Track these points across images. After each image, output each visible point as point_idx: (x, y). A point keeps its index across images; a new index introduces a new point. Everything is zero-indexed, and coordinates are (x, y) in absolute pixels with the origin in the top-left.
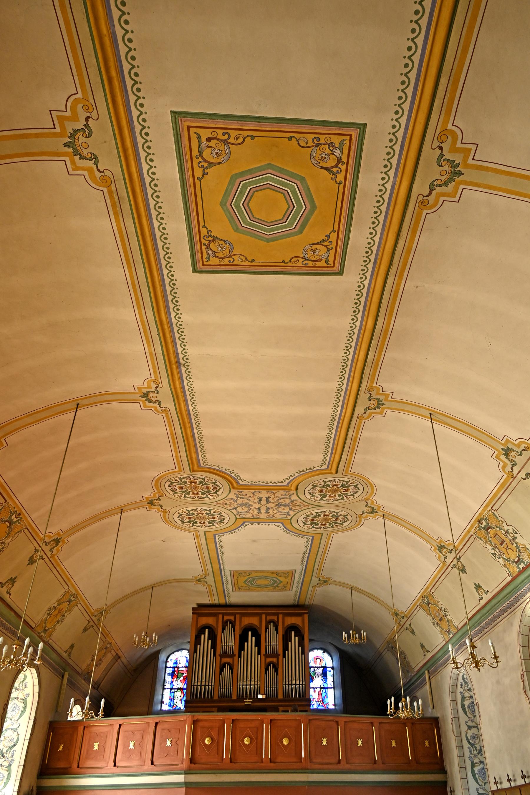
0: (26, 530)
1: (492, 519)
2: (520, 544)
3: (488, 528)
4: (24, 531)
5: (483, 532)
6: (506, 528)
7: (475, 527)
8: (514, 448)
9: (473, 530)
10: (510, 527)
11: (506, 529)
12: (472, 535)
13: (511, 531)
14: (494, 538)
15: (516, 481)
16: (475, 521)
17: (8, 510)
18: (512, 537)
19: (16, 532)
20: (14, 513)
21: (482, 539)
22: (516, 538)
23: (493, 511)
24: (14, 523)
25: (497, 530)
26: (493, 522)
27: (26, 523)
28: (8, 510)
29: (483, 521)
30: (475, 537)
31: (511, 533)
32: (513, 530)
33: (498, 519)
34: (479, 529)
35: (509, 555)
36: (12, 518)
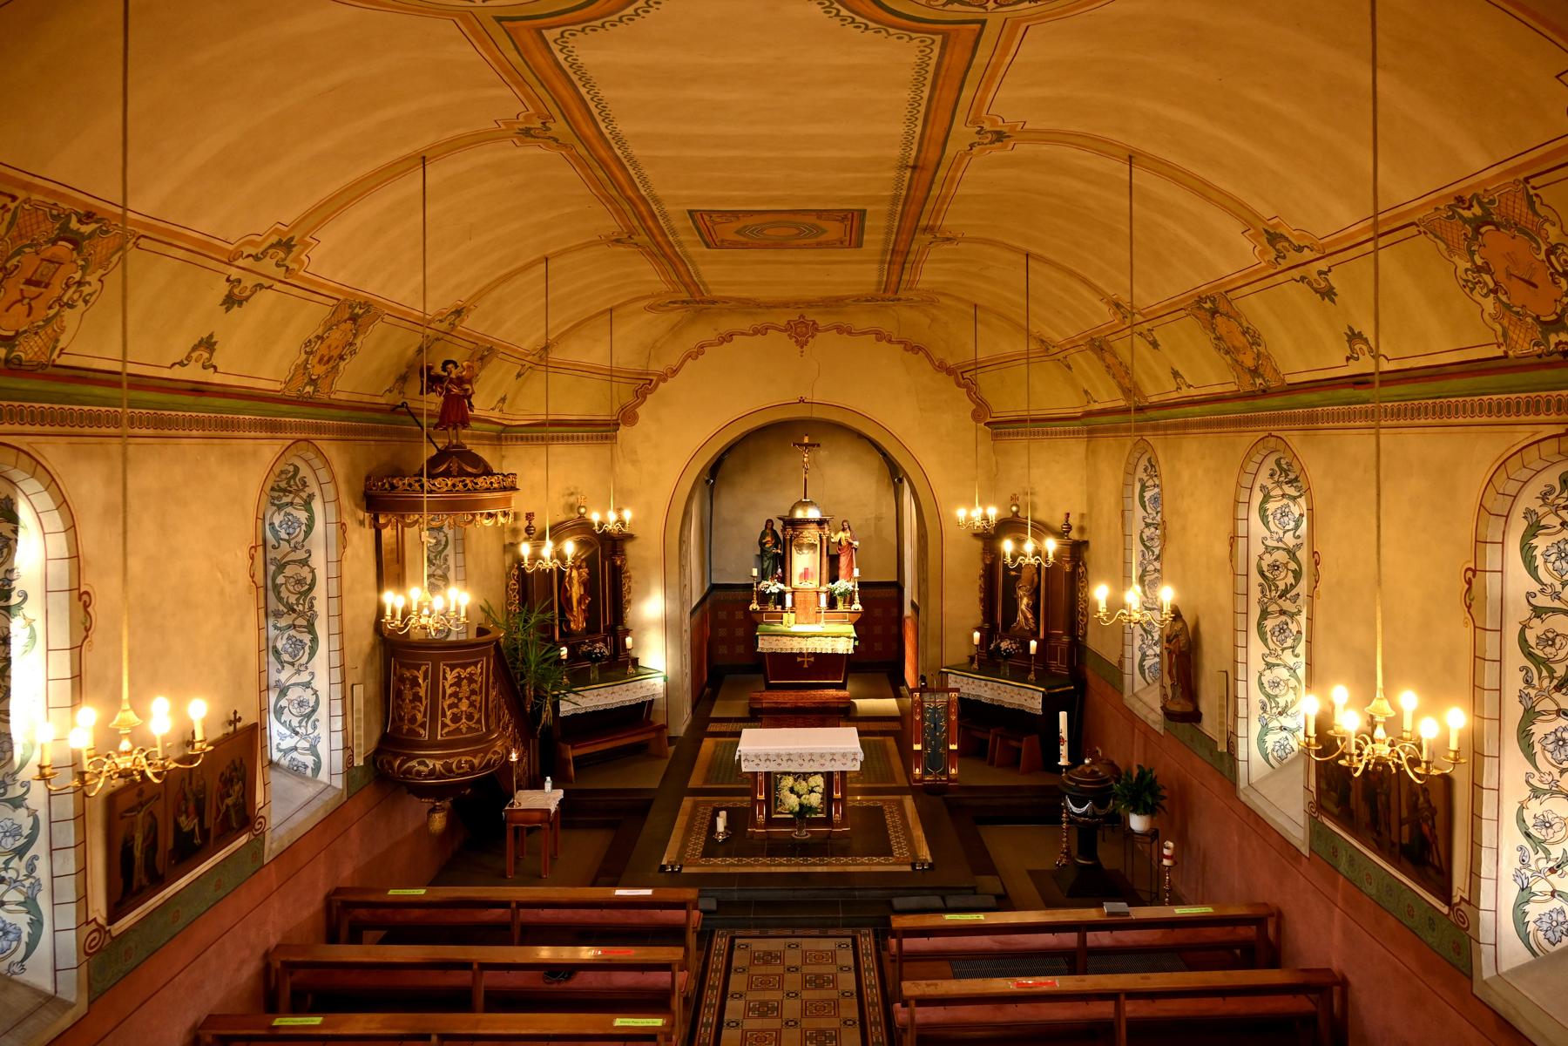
0: (1533, 182)
1: (110, 245)
2: (62, 321)
3: (76, 241)
4: (1534, 188)
5: (52, 228)
6: (92, 279)
7: (55, 204)
8: (291, 256)
9: (35, 197)
10: (96, 285)
11: (88, 279)
12: (14, 198)
13: (86, 290)
14: (43, 260)
15: (221, 267)
16: (85, 204)
17: (1442, 222)
18: (71, 298)
19: (1525, 210)
20: (1454, 212)
21: (15, 228)
22: (71, 306)
23: (134, 240)
24: (1488, 213)
25: (75, 262)
26: (101, 247)
27: (1506, 181)
28: (1442, 222)
29: (93, 226)
30: (12, 206)
31: (82, 292)
32: (91, 295)
33: (112, 255)
34: (52, 216)
35: (7, 310)
36: (1471, 216)
